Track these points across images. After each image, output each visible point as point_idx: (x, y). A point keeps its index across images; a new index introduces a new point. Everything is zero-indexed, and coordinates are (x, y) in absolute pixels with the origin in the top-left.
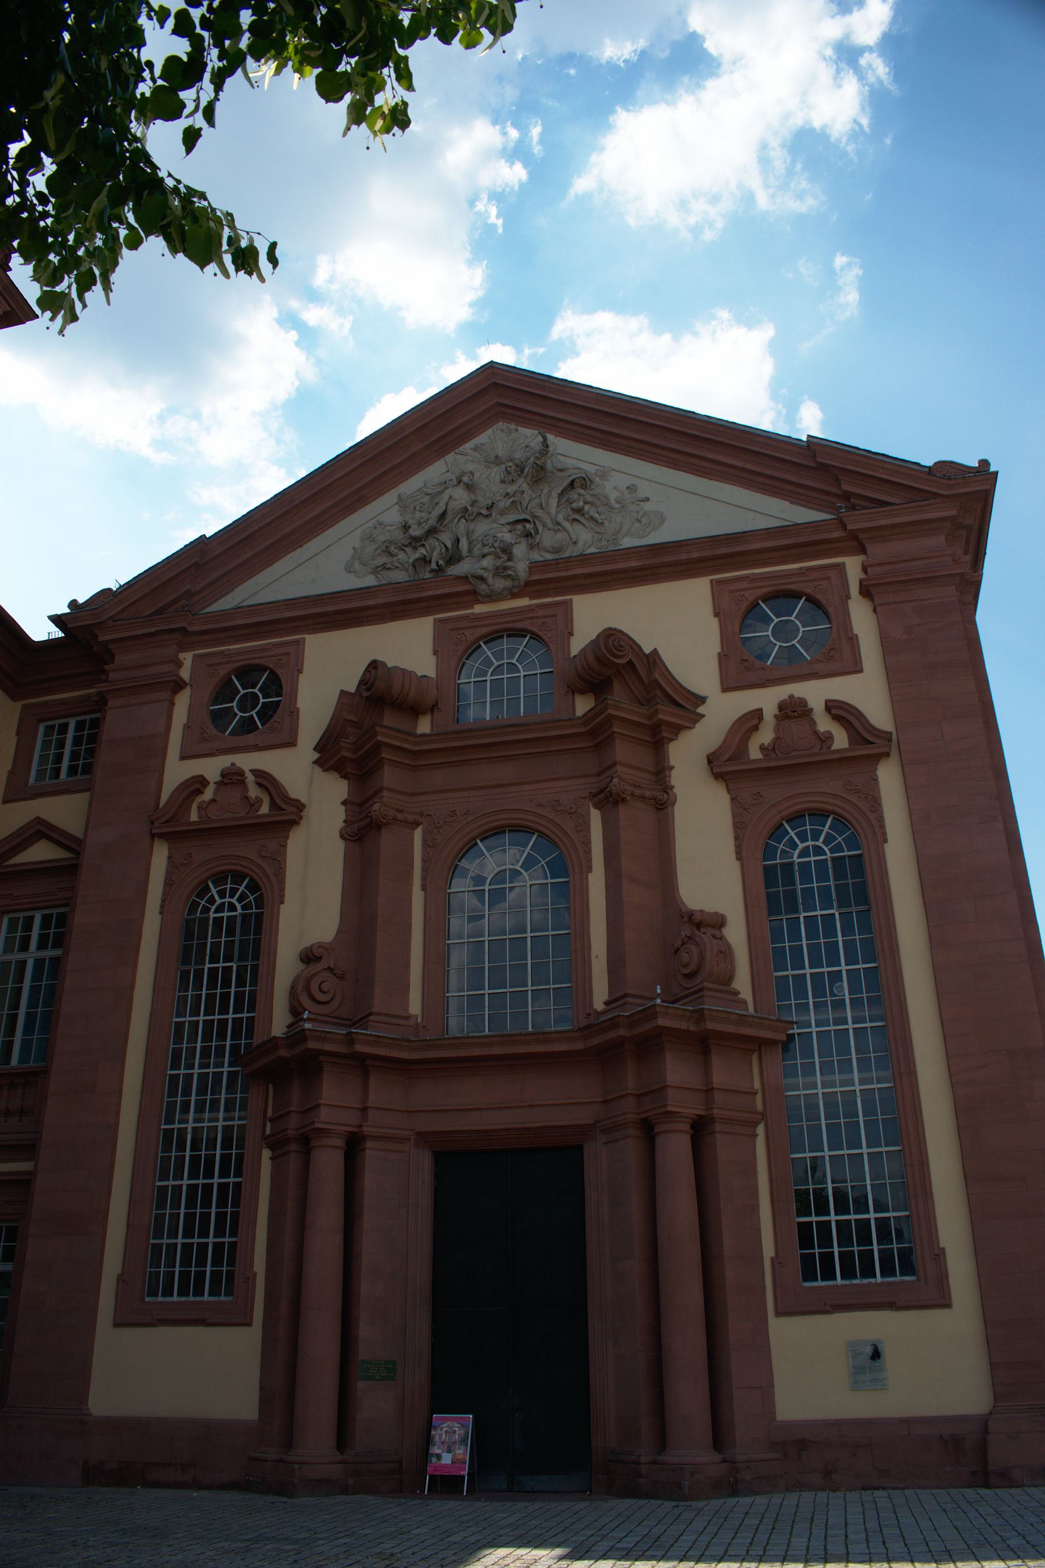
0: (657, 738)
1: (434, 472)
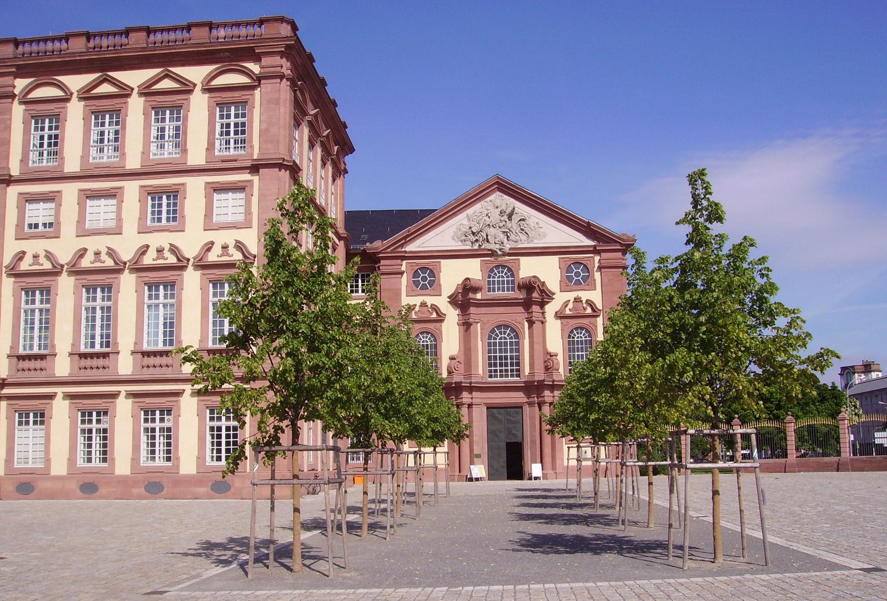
0: (542, 304)
1: (477, 207)
